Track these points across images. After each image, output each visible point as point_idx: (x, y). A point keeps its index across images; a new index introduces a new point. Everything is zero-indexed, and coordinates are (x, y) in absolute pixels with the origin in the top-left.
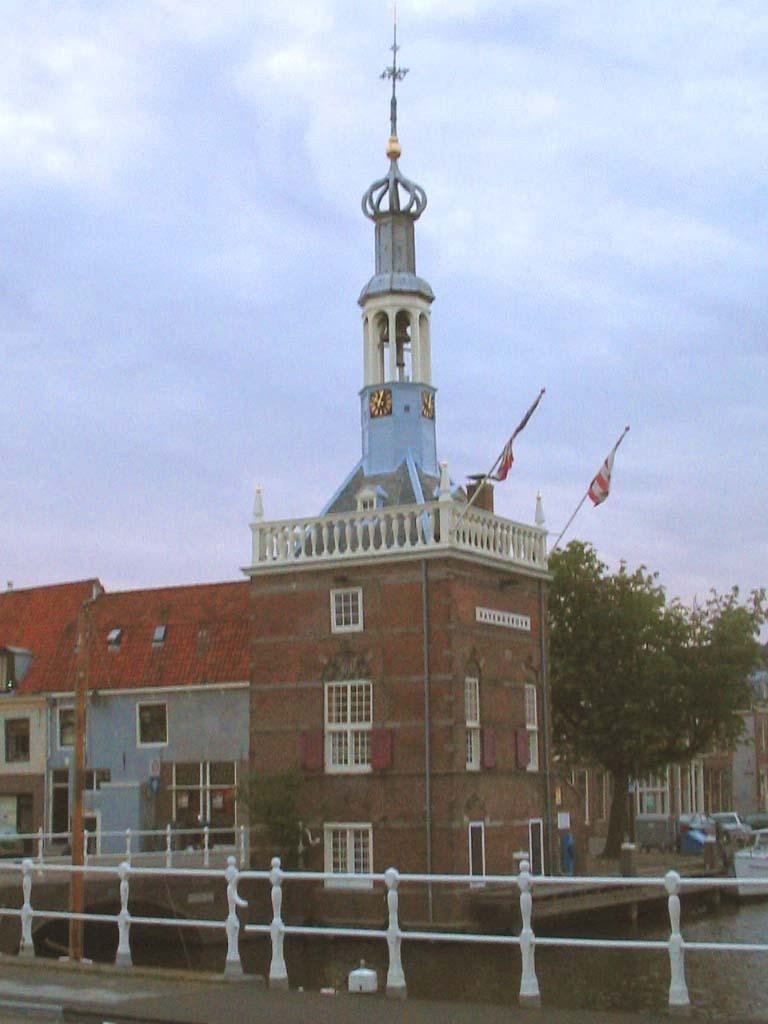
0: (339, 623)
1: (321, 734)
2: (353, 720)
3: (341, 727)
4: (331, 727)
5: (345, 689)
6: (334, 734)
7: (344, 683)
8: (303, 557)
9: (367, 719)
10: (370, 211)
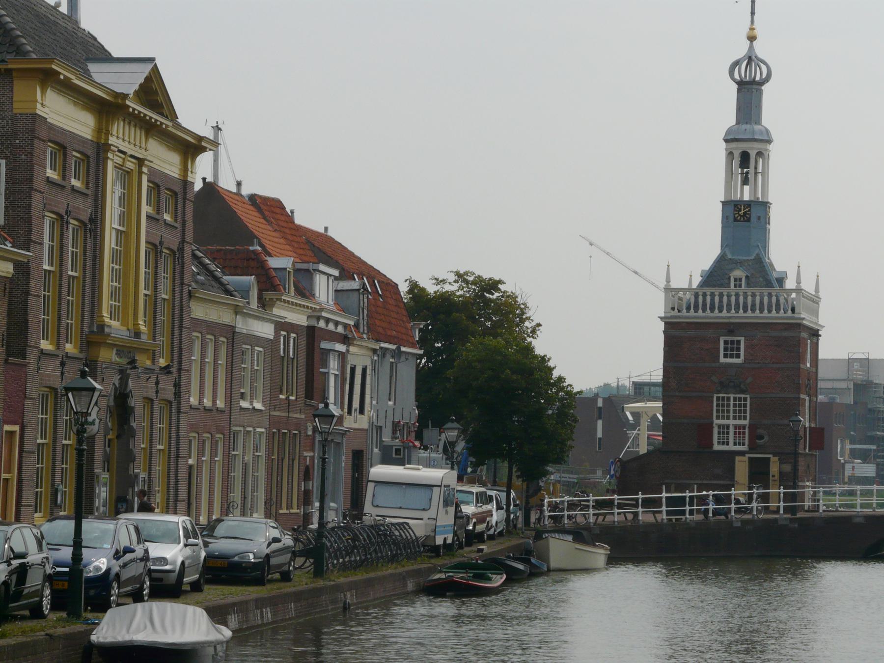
0: (726, 356)
1: (710, 426)
2: (734, 418)
4: (716, 422)
5: (729, 399)
6: (719, 426)
8: (684, 312)
10: (737, 76)
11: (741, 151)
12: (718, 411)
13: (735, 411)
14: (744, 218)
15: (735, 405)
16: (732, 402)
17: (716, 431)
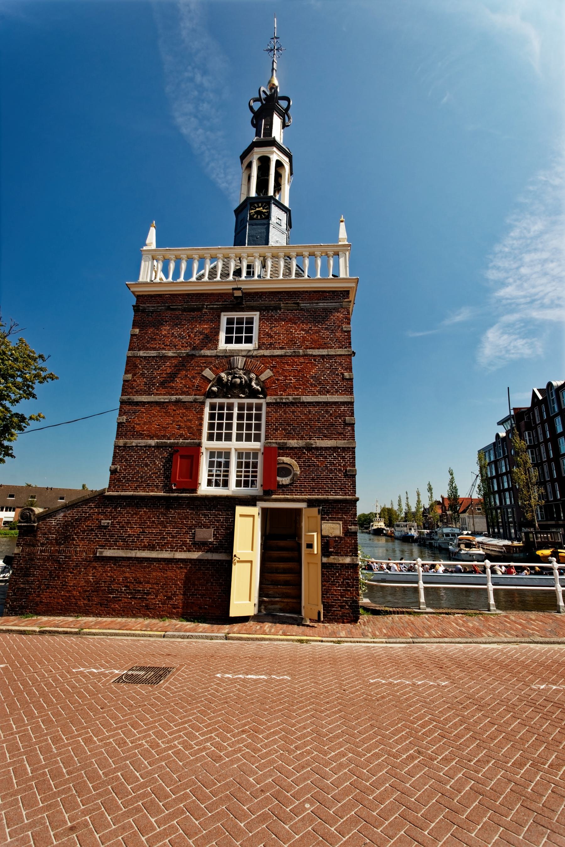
0: (229, 340)
3: (222, 445)
5: (230, 407)
7: (231, 401)
9: (257, 438)
12: (211, 427)
13: (240, 427)
14: (261, 217)
15: (240, 417)
16: (236, 411)
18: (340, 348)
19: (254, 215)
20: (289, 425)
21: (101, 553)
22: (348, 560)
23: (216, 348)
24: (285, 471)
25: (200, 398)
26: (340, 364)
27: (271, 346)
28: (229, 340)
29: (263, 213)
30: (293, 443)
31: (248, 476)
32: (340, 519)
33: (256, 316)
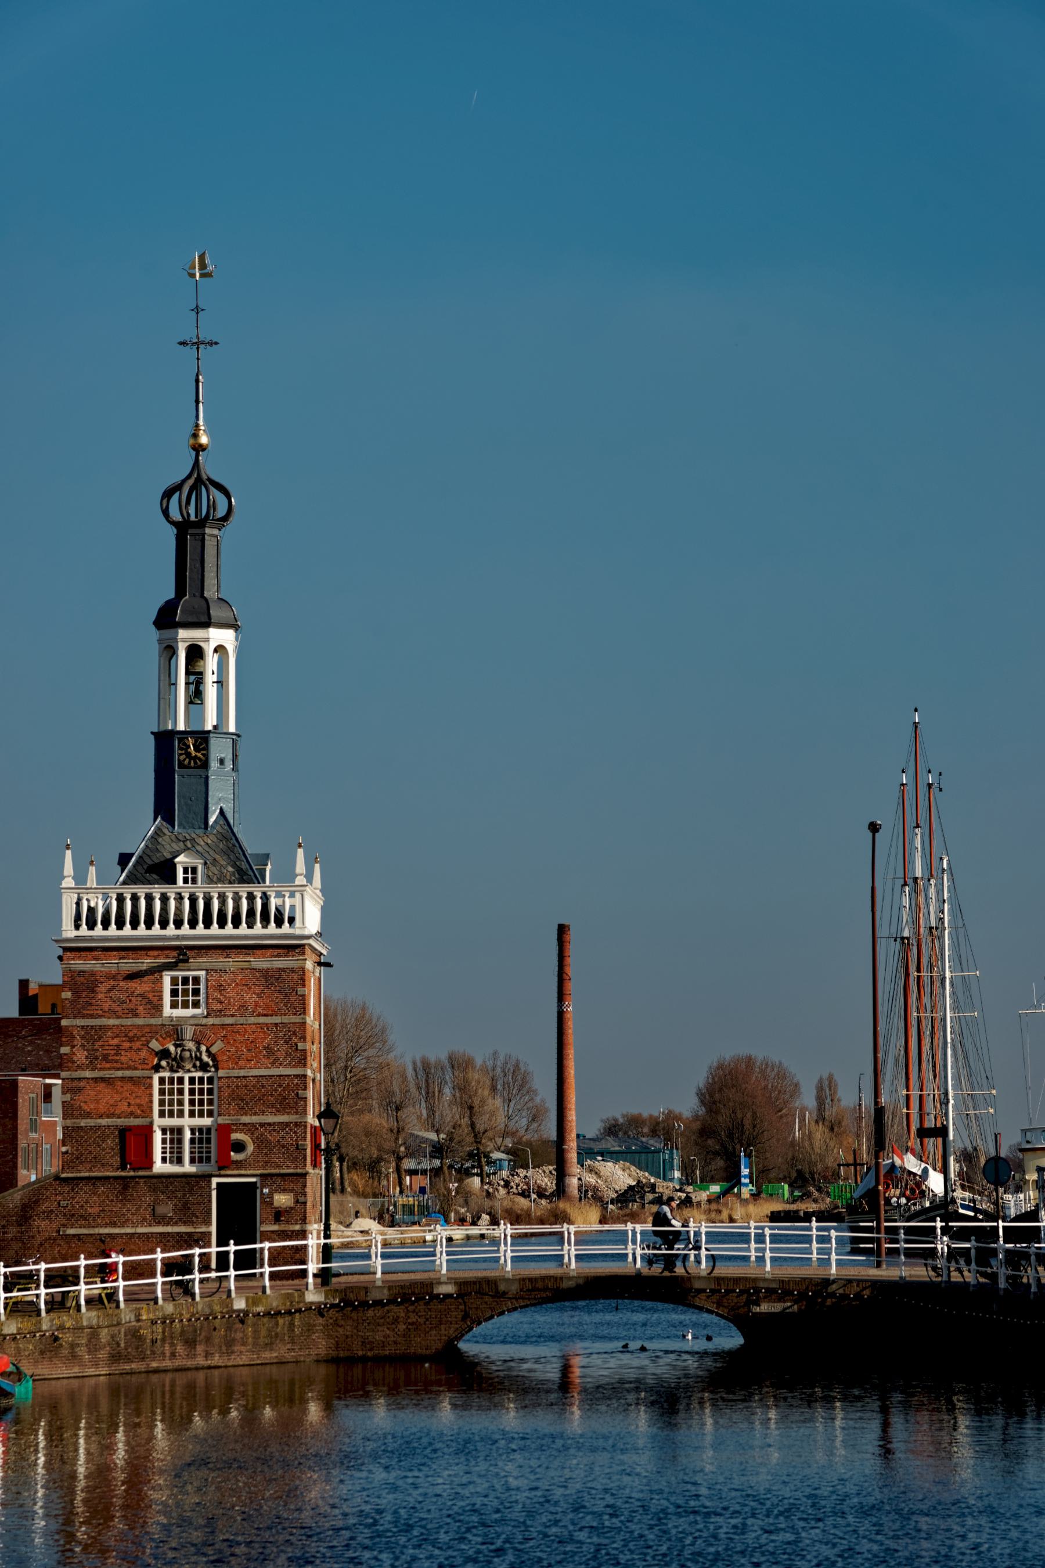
2: (192, 1114)
3: (175, 1122)
4: (158, 1122)
10: (175, 515)
11: (188, 644)
12: (162, 1103)
13: (192, 1102)
14: (195, 763)
15: (192, 1092)
16: (187, 1086)
17: (158, 1136)
18: (295, 1014)
19: (184, 760)
20: (242, 1100)
21: (64, 1231)
22: (297, 1227)
23: (161, 1016)
24: (240, 1147)
25: (146, 1073)
26: (295, 1033)
27: (220, 1013)
28: (174, 1005)
29: (200, 759)
30: (246, 1119)
31: (202, 1152)
32: (291, 1191)
33: (202, 974)
